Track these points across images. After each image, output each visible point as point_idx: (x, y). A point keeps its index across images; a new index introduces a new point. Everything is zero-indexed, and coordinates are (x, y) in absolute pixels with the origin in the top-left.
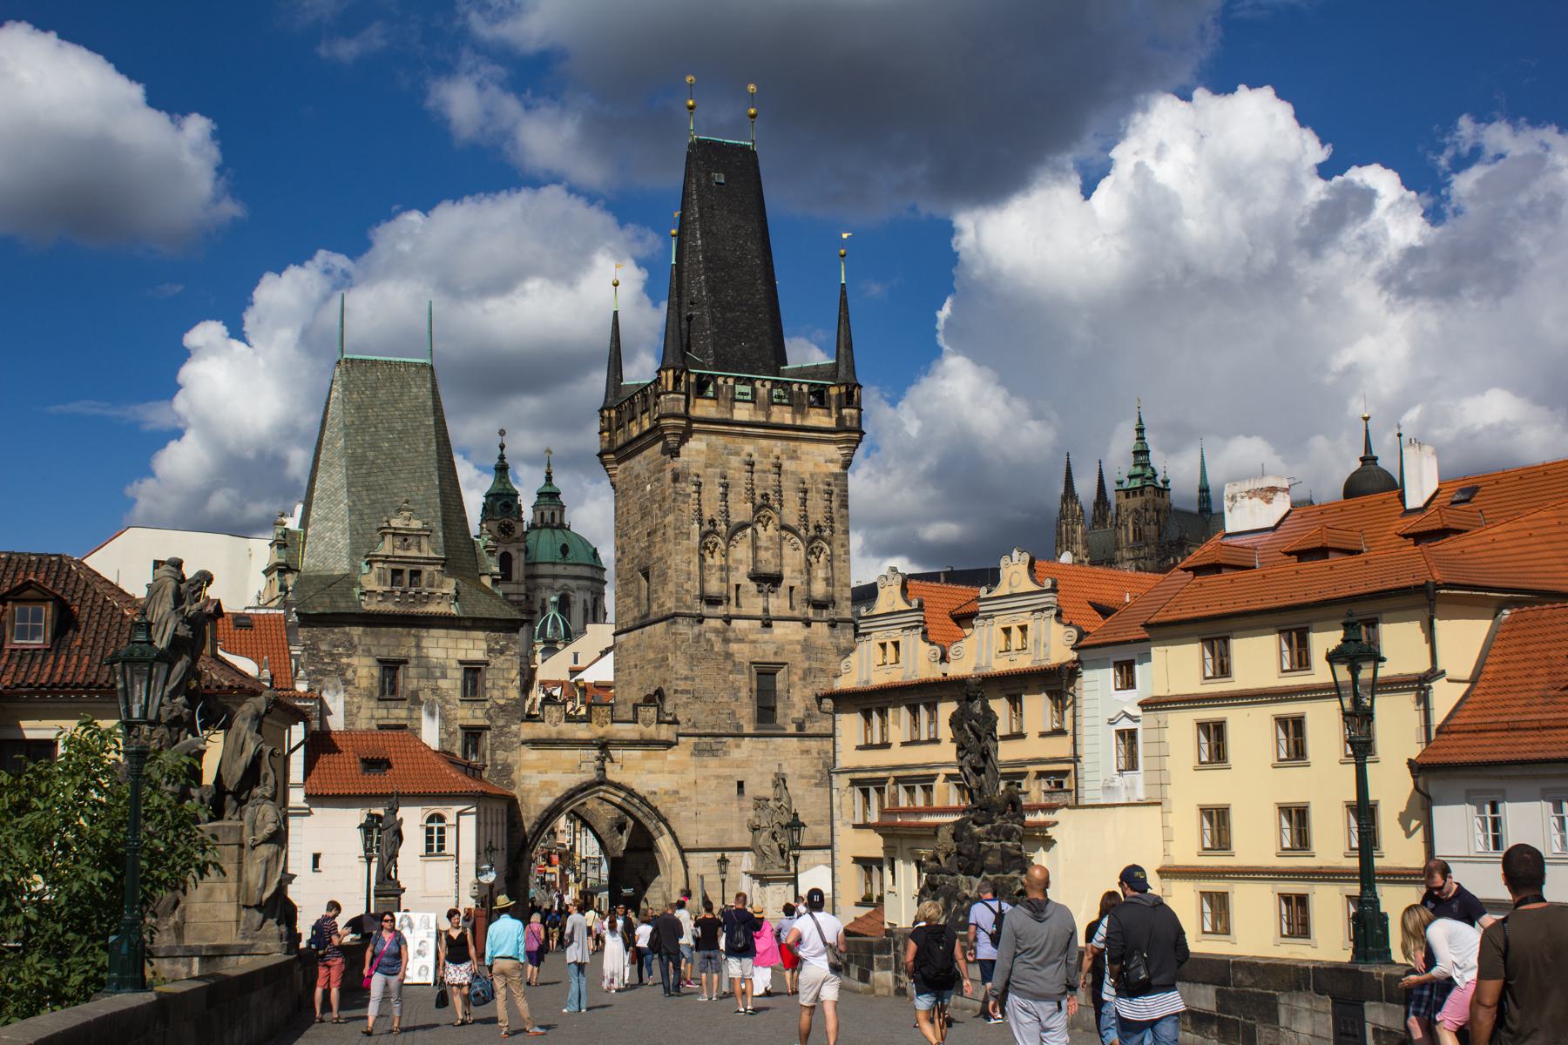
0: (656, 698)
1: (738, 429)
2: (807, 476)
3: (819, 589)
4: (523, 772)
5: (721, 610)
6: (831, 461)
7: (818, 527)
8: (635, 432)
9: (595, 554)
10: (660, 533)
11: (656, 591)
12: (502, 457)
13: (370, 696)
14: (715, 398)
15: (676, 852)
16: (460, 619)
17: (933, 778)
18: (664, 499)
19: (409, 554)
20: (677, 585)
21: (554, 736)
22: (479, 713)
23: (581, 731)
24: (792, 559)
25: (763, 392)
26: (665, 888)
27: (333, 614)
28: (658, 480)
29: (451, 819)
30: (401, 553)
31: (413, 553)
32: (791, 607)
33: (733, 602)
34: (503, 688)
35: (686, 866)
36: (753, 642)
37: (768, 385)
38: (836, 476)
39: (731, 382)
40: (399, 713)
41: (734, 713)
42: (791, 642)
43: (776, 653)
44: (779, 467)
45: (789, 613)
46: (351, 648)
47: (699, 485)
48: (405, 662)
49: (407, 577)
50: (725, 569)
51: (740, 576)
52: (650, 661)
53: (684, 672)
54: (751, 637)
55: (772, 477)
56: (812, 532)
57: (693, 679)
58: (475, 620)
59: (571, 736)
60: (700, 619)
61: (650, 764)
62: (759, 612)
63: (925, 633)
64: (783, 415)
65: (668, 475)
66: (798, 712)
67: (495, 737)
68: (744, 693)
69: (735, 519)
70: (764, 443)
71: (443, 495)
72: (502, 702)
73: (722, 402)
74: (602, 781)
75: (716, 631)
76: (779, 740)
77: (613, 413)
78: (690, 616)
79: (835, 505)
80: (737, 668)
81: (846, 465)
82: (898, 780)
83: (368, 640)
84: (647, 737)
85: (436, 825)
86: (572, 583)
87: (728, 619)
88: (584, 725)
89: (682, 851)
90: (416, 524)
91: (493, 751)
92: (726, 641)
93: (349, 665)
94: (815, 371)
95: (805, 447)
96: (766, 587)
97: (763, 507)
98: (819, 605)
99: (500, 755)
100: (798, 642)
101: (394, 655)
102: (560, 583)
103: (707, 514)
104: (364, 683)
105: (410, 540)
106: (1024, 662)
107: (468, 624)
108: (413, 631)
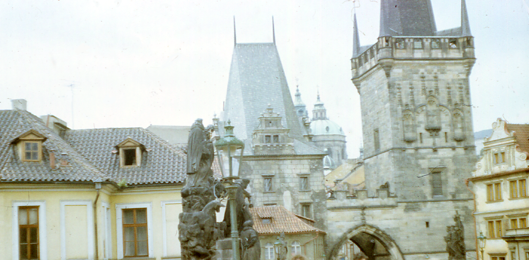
0: (386, 187)
1: (417, 61)
2: (450, 81)
3: (458, 132)
4: (329, 222)
5: (413, 145)
6: (461, 73)
8: (368, 68)
9: (341, 130)
10: (383, 112)
12: (298, 90)
13: (260, 191)
14: (405, 48)
16: (297, 156)
19: (271, 128)
21: (342, 205)
23: (354, 203)
24: (445, 120)
25: (427, 43)
28: (380, 88)
31: (274, 128)
32: (446, 141)
33: (419, 141)
36: (430, 158)
37: (429, 41)
38: (464, 80)
39: (412, 40)
40: (272, 198)
43: (440, 163)
44: (436, 77)
45: (444, 144)
48: (273, 176)
49: (272, 138)
51: (421, 129)
53: (398, 172)
54: (429, 156)
55: (433, 83)
56: (454, 107)
60: (404, 150)
63: (517, 147)
64: (437, 54)
65: (386, 87)
67: (316, 207)
69: (417, 104)
70: (429, 67)
71: (285, 101)
72: (317, 192)
73: (408, 50)
75: (412, 155)
76: (444, 203)
77: (357, 61)
79: (464, 93)
80: (423, 170)
82: (509, 216)
83: (257, 167)
84: (383, 204)
87: (417, 149)
91: (315, 213)
92: (417, 159)
94: (451, 32)
95: (448, 68)
96: (434, 133)
97: (431, 96)
98: (459, 141)
102: (326, 143)
108: (277, 162)
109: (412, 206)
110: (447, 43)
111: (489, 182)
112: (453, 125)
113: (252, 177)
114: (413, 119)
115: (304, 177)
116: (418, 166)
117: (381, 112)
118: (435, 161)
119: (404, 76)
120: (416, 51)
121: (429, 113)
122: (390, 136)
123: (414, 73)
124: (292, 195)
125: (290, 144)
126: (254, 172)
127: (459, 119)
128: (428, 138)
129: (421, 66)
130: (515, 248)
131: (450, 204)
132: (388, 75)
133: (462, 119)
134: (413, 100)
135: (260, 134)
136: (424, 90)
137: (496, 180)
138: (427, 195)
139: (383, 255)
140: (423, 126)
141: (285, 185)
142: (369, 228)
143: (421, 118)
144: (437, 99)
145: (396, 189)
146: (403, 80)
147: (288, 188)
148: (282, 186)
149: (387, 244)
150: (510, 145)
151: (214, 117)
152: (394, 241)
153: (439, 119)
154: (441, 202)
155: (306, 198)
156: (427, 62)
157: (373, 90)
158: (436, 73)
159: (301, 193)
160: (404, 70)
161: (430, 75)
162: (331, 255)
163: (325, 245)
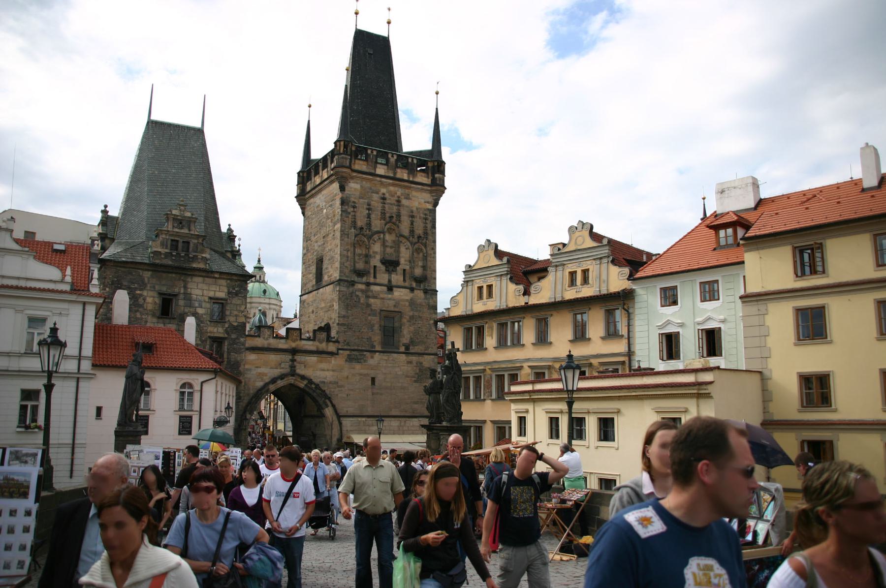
1: (378, 179)
2: (415, 209)
3: (418, 272)
4: (247, 367)
5: (364, 279)
9: (278, 294)
10: (331, 236)
13: (154, 315)
14: (366, 160)
15: (335, 418)
16: (212, 272)
17: (521, 368)
19: (182, 231)
20: (342, 264)
21: (266, 346)
22: (221, 330)
23: (282, 344)
24: (405, 255)
25: (393, 160)
27: (132, 263)
28: (331, 206)
29: (197, 387)
30: (177, 230)
31: (185, 231)
32: (404, 280)
34: (236, 316)
35: (340, 424)
36: (383, 299)
37: (395, 157)
39: (375, 153)
41: (369, 339)
43: (395, 306)
44: (399, 201)
45: (401, 283)
46: (143, 286)
47: (354, 207)
48: (175, 295)
50: (367, 256)
51: (376, 261)
52: (322, 308)
53: (343, 313)
54: (382, 296)
57: (348, 317)
58: (221, 273)
60: (353, 283)
61: (323, 365)
62: (386, 282)
63: (511, 279)
64: (403, 174)
65: (338, 202)
66: (405, 339)
67: (229, 344)
68: (376, 327)
69: (374, 229)
70: (392, 188)
72: (235, 324)
74: (293, 373)
75: (362, 291)
76: (395, 355)
79: (429, 226)
80: (373, 313)
81: (436, 204)
82: (492, 370)
83: (154, 281)
84: (321, 349)
85: (187, 390)
86: (267, 306)
88: (283, 341)
89: (339, 417)
90: (188, 214)
91: (229, 353)
92: (368, 297)
93: (141, 295)
94: (420, 153)
95: (414, 193)
96: (391, 268)
99: (234, 356)
100: (407, 300)
101: (169, 291)
104: (150, 307)
105: (184, 223)
106: (587, 292)
107: (216, 276)
109: (356, 355)
111: (468, 324)
112: (411, 261)
113: (145, 293)
114: (368, 248)
115: (221, 303)
116: (368, 305)
117: (328, 235)
120: (378, 166)
121: (387, 244)
122: (337, 265)
124: (198, 325)
127: (421, 254)
129: (382, 183)
130: (527, 411)
131: (403, 357)
132: (342, 188)
133: (425, 258)
134: (369, 224)
135: (164, 236)
136: (383, 213)
137: (479, 323)
138: (375, 344)
139: (313, 417)
140: (378, 257)
143: (377, 247)
144: (398, 227)
145: (338, 332)
147: (195, 314)
148: (186, 310)
149: (321, 402)
150: (501, 275)
152: (329, 399)
153: (398, 251)
155: (218, 331)
157: (322, 209)
158: (399, 197)
159: (212, 324)
162: (245, 412)
163: (239, 398)
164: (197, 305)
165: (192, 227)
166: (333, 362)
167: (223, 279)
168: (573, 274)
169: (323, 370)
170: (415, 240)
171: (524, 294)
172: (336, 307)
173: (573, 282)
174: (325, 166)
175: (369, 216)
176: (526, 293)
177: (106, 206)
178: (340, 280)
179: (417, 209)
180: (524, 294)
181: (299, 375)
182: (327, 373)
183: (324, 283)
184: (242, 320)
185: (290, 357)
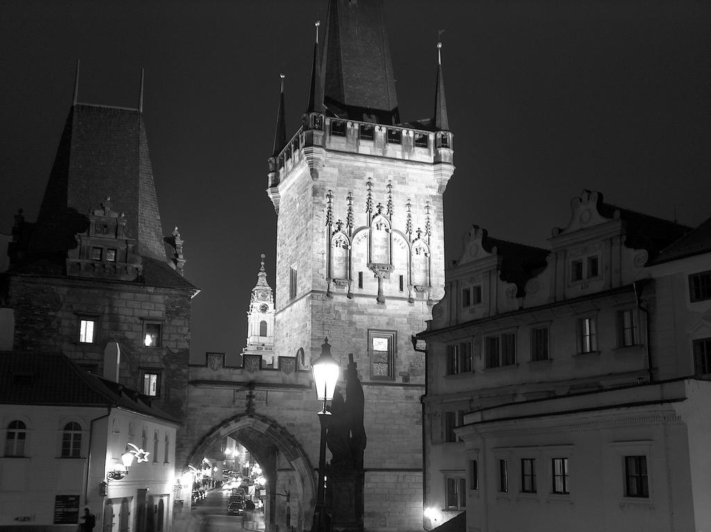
1: (362, 159)
2: (412, 197)
3: (419, 278)
4: (190, 405)
6: (431, 187)
7: (419, 232)
10: (304, 235)
11: (300, 278)
18: (307, 210)
21: (215, 379)
23: (237, 376)
26: (301, 497)
29: (85, 426)
32: (401, 289)
34: (177, 341)
36: (371, 314)
39: (356, 126)
42: (400, 316)
43: (388, 324)
47: (330, 196)
48: (99, 316)
53: (319, 334)
54: (370, 311)
59: (229, 379)
60: (329, 294)
65: (310, 192)
72: (176, 351)
73: (351, 140)
74: (250, 411)
75: (343, 305)
76: (390, 388)
77: (278, 162)
78: (322, 292)
80: (358, 333)
84: (288, 382)
85: (72, 432)
92: (351, 313)
93: (54, 317)
100: (405, 316)
103: (335, 220)
106: (597, 286)
110: (410, 138)
112: (410, 265)
116: (352, 323)
118: (379, 318)
119: (339, 179)
120: (362, 142)
123: (356, 178)
125: (135, 266)
126: (64, 308)
128: (371, 281)
140: (365, 261)
141: (118, 334)
142: (259, 422)
146: (338, 186)
148: (112, 335)
151: (17, 214)
154: (386, 387)
156: (379, 162)
160: (339, 170)
161: (381, 184)
164: (126, 328)
165: (120, 231)
166: (304, 398)
167: (160, 294)
168: (578, 266)
169: (293, 409)
170: (414, 236)
171: (518, 296)
172: (309, 327)
173: (578, 276)
174: (297, 147)
175: (350, 209)
176: (521, 293)
177: (21, 211)
178: (312, 291)
179: (416, 196)
180: (518, 296)
181: (259, 415)
182: (296, 413)
183: (297, 297)
184: (186, 345)
185: (247, 392)
